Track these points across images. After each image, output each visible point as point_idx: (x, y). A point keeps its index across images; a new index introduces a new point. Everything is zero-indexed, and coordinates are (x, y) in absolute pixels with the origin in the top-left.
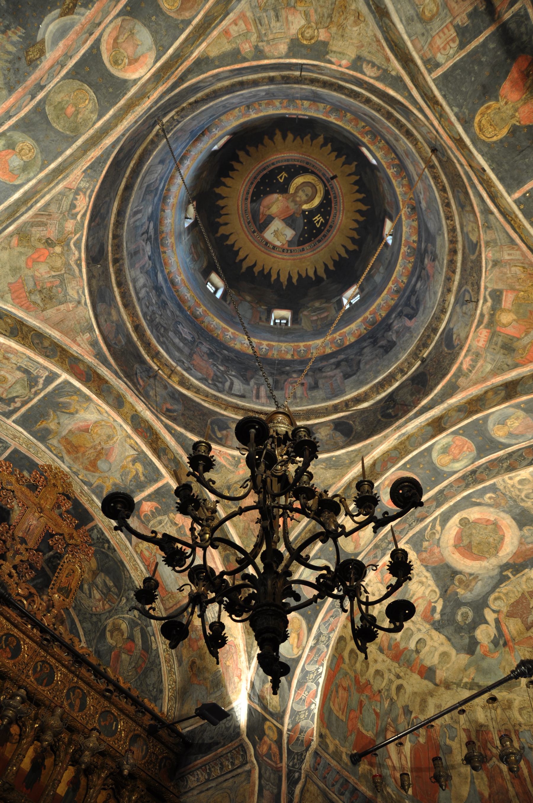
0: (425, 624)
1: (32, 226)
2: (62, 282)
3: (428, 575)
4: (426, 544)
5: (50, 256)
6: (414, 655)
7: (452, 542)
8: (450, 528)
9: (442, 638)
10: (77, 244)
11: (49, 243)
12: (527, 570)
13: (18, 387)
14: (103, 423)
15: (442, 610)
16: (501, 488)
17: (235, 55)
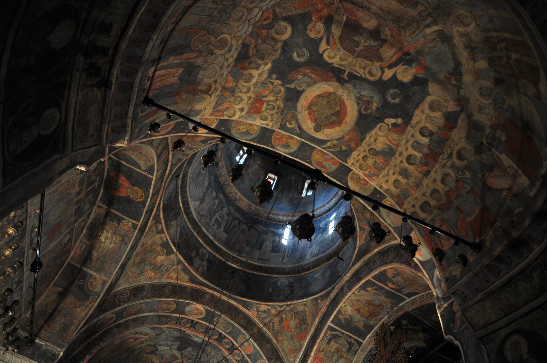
0: (407, 131)
1: (273, 330)
2: (297, 313)
3: (368, 137)
4: (344, 148)
5: (286, 320)
6: (434, 137)
7: (337, 129)
8: (326, 135)
9: (417, 112)
10: (281, 307)
11: (281, 321)
12: (335, 65)
13: (341, 342)
14: (351, 304)
15: (394, 118)
16: (279, 124)
17: (185, 269)
